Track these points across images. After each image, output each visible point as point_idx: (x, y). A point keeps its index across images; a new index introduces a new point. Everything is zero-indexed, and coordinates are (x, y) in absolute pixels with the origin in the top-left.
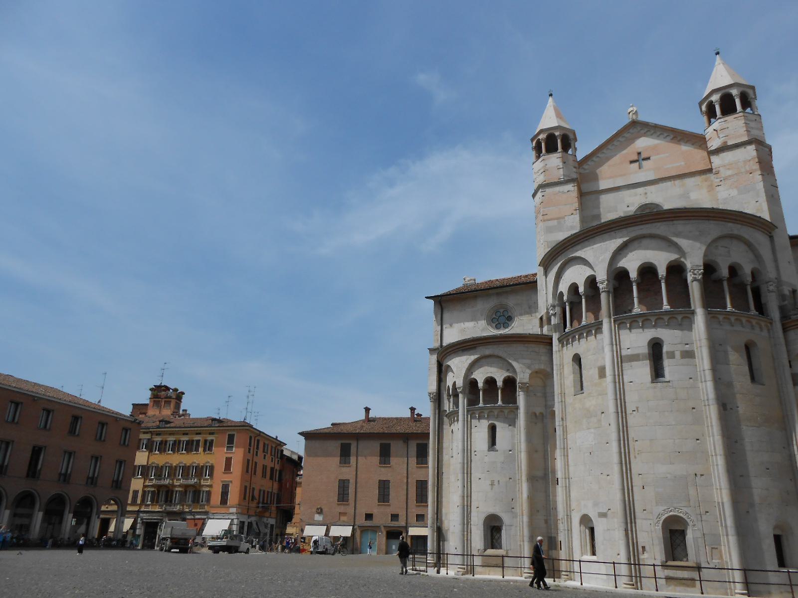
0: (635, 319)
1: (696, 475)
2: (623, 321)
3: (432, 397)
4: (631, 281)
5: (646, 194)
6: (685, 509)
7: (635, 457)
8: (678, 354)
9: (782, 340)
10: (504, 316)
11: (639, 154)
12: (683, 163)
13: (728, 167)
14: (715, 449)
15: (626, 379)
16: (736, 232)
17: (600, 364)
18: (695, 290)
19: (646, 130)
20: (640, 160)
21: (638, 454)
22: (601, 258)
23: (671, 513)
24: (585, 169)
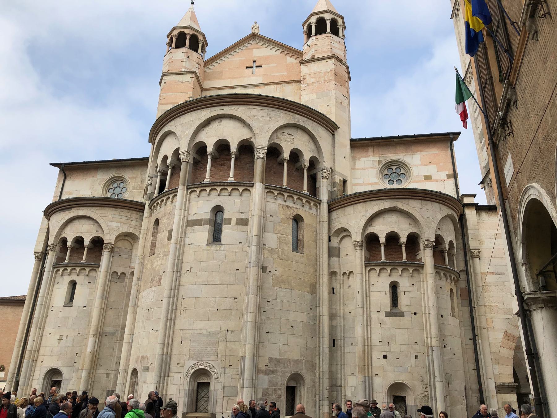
0: (204, 188)
3: (37, 256)
4: (207, 154)
6: (212, 363)
7: (180, 313)
8: (234, 221)
9: (326, 219)
10: (120, 187)
11: (254, 61)
13: (312, 76)
14: (247, 307)
15: (188, 241)
16: (301, 123)
17: (170, 228)
18: (259, 165)
19: (262, 43)
20: (254, 66)
21: (183, 311)
22: (186, 132)
23: (200, 367)
24: (210, 69)
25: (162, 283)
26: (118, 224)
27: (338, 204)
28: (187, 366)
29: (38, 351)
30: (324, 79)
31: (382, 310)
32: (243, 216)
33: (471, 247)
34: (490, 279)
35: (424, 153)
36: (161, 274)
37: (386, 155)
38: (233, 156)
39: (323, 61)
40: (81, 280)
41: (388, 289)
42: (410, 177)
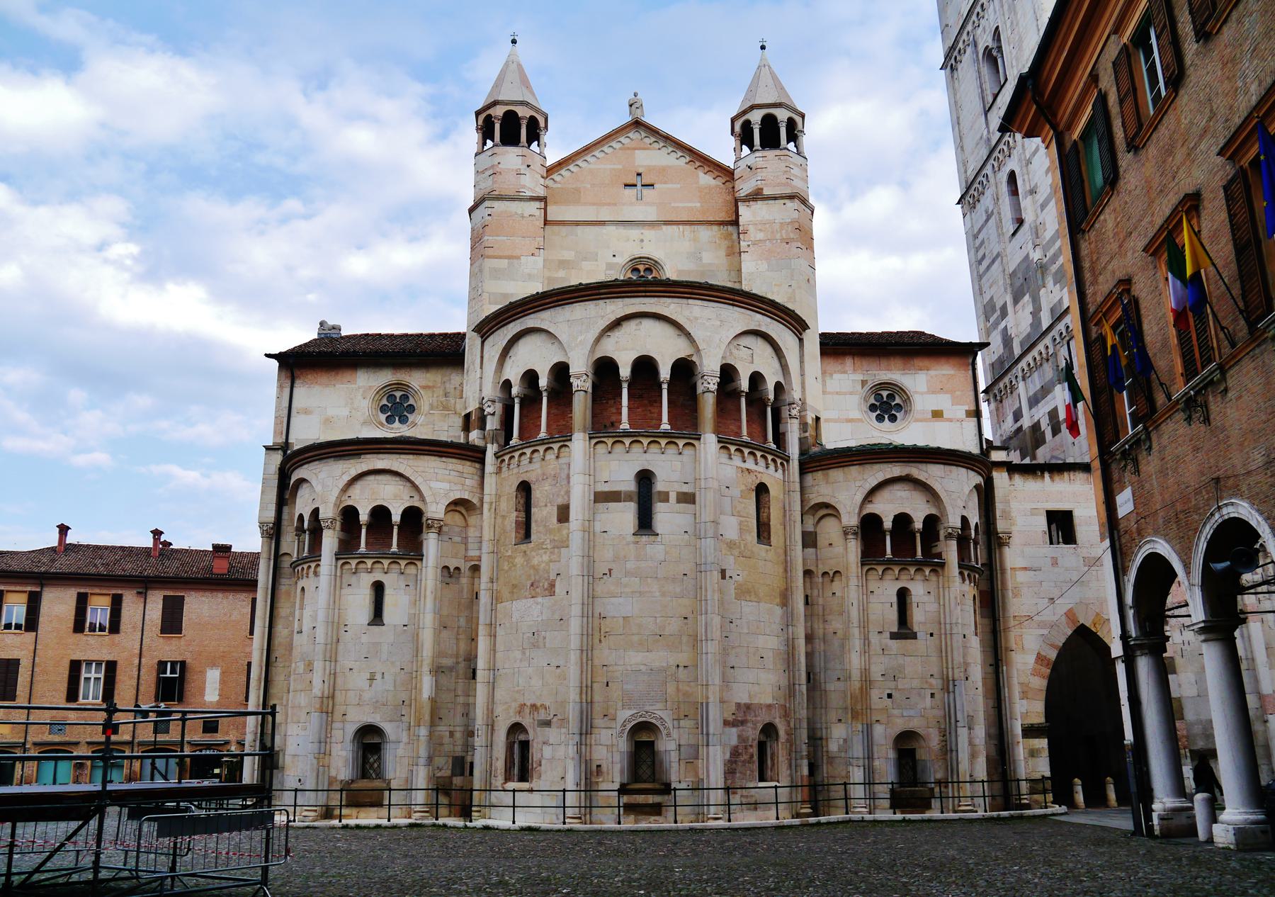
1: (678, 666)
2: (602, 439)
5: (642, 241)
6: (659, 713)
7: (600, 641)
8: (673, 497)
12: (698, 205)
13: (760, 227)
14: (706, 632)
15: (598, 527)
17: (560, 501)
20: (639, 185)
25: (557, 590)
26: (446, 486)
27: (818, 464)
28: (620, 720)
29: (333, 697)
30: (782, 236)
31: (886, 629)
32: (685, 489)
33: (999, 530)
34: (1021, 577)
35: (932, 373)
36: (552, 576)
37: (874, 372)
38: (665, 386)
39: (777, 201)
40: (392, 582)
41: (894, 599)
42: (910, 410)
